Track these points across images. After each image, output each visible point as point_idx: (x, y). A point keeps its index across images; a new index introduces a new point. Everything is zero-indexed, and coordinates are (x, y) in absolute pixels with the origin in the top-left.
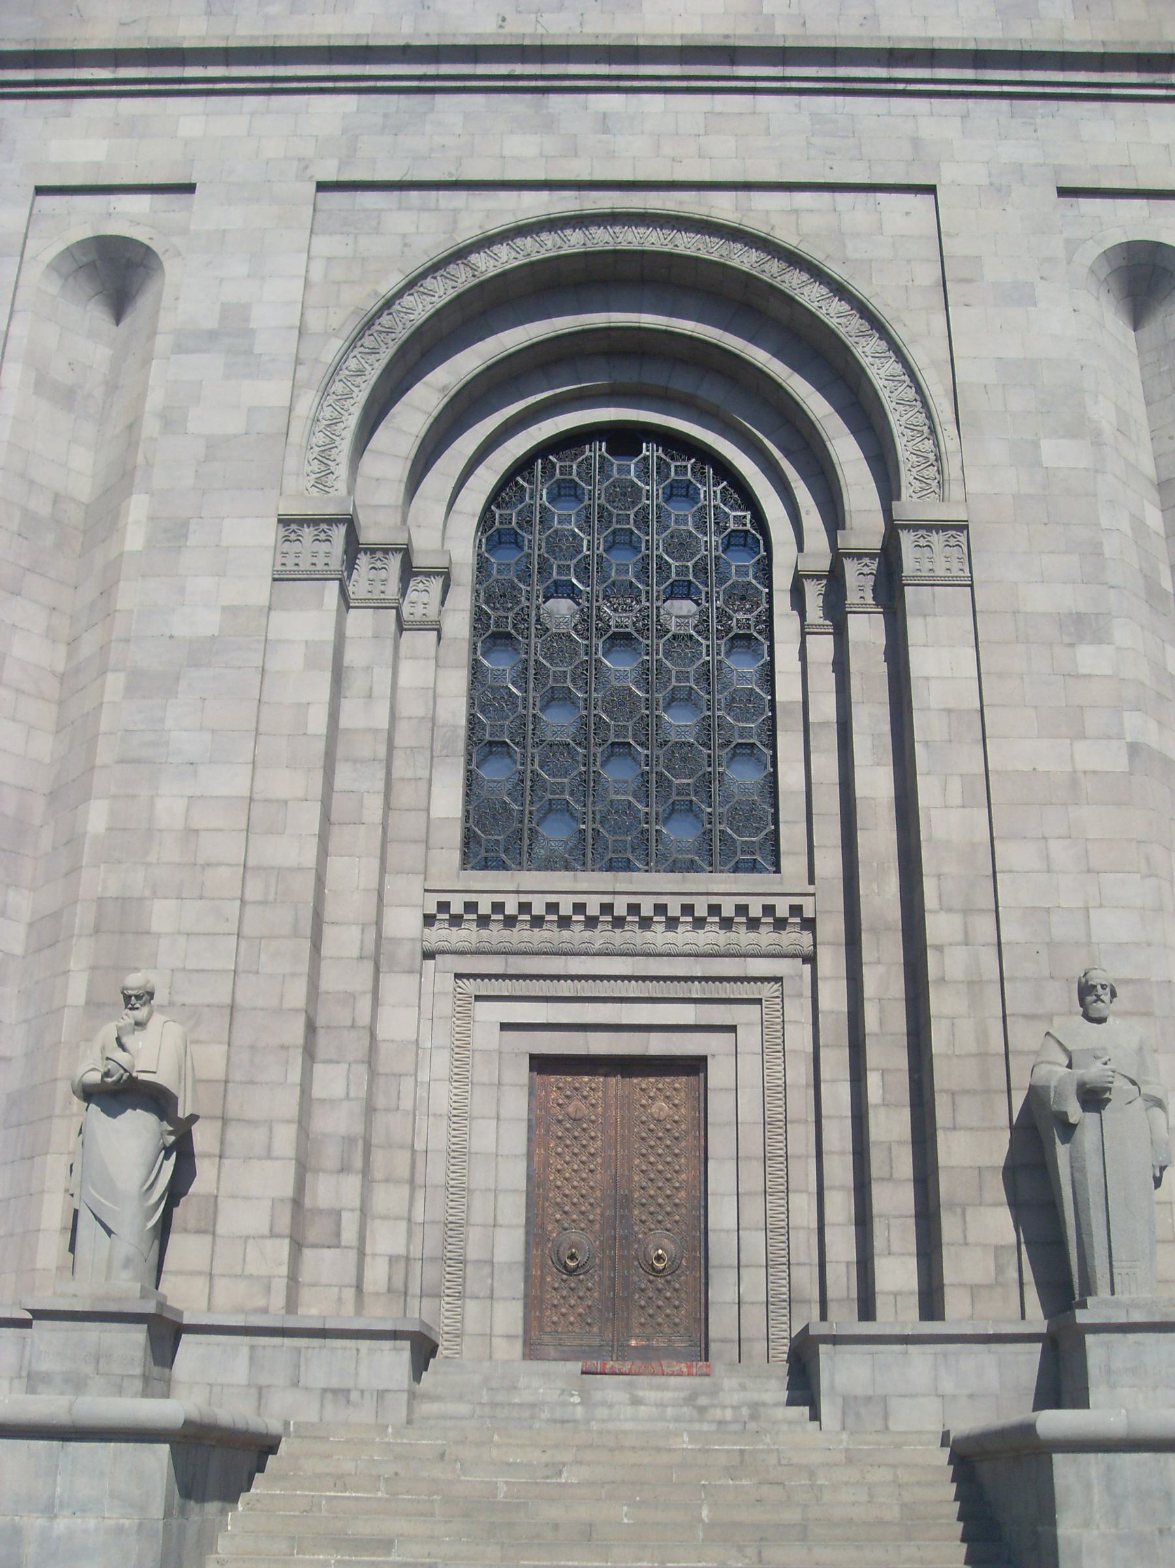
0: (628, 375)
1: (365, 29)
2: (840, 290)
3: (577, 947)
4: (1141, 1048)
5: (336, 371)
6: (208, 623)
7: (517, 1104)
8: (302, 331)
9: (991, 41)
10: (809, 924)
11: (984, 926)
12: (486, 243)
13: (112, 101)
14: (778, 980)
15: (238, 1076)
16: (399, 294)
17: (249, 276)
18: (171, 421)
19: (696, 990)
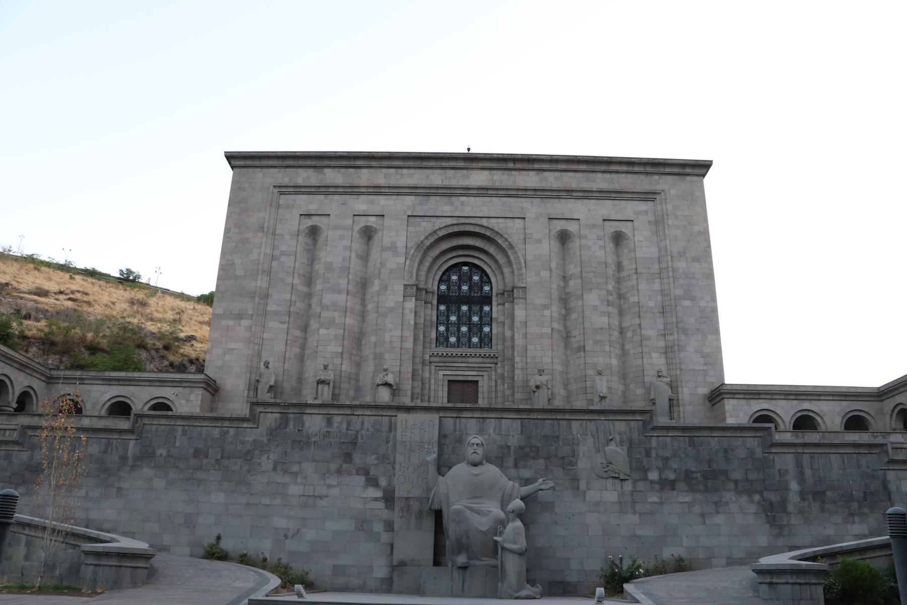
0: (466, 253)
1: (416, 183)
2: (506, 240)
3: (456, 361)
4: (547, 380)
5: (413, 256)
6: (392, 304)
7: (446, 388)
8: (406, 247)
9: (538, 187)
11: (524, 360)
12: (440, 229)
13: (366, 196)
15: (401, 383)
16: (424, 240)
17: (396, 236)
18: (382, 264)
19: (477, 369)
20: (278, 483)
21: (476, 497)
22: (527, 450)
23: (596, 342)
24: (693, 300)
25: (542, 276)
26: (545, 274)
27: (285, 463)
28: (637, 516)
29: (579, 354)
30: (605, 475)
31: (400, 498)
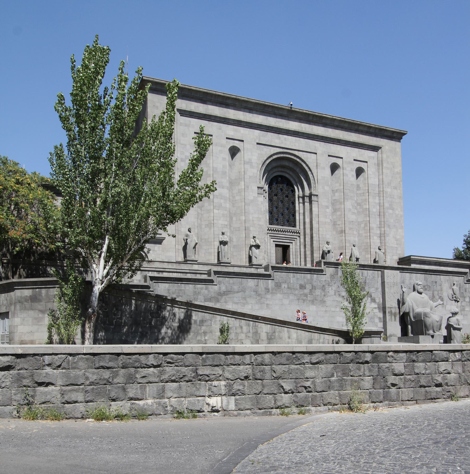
0: (283, 170)
6: (252, 198)
7: (274, 248)
10: (299, 233)
14: (296, 238)
19: (290, 239)
20: (337, 301)
21: (424, 307)
22: (426, 287)
23: (350, 229)
24: (393, 210)
25: (325, 189)
26: (327, 188)
27: (339, 291)
28: (462, 316)
29: (341, 234)
30: (452, 299)
31: (389, 308)
